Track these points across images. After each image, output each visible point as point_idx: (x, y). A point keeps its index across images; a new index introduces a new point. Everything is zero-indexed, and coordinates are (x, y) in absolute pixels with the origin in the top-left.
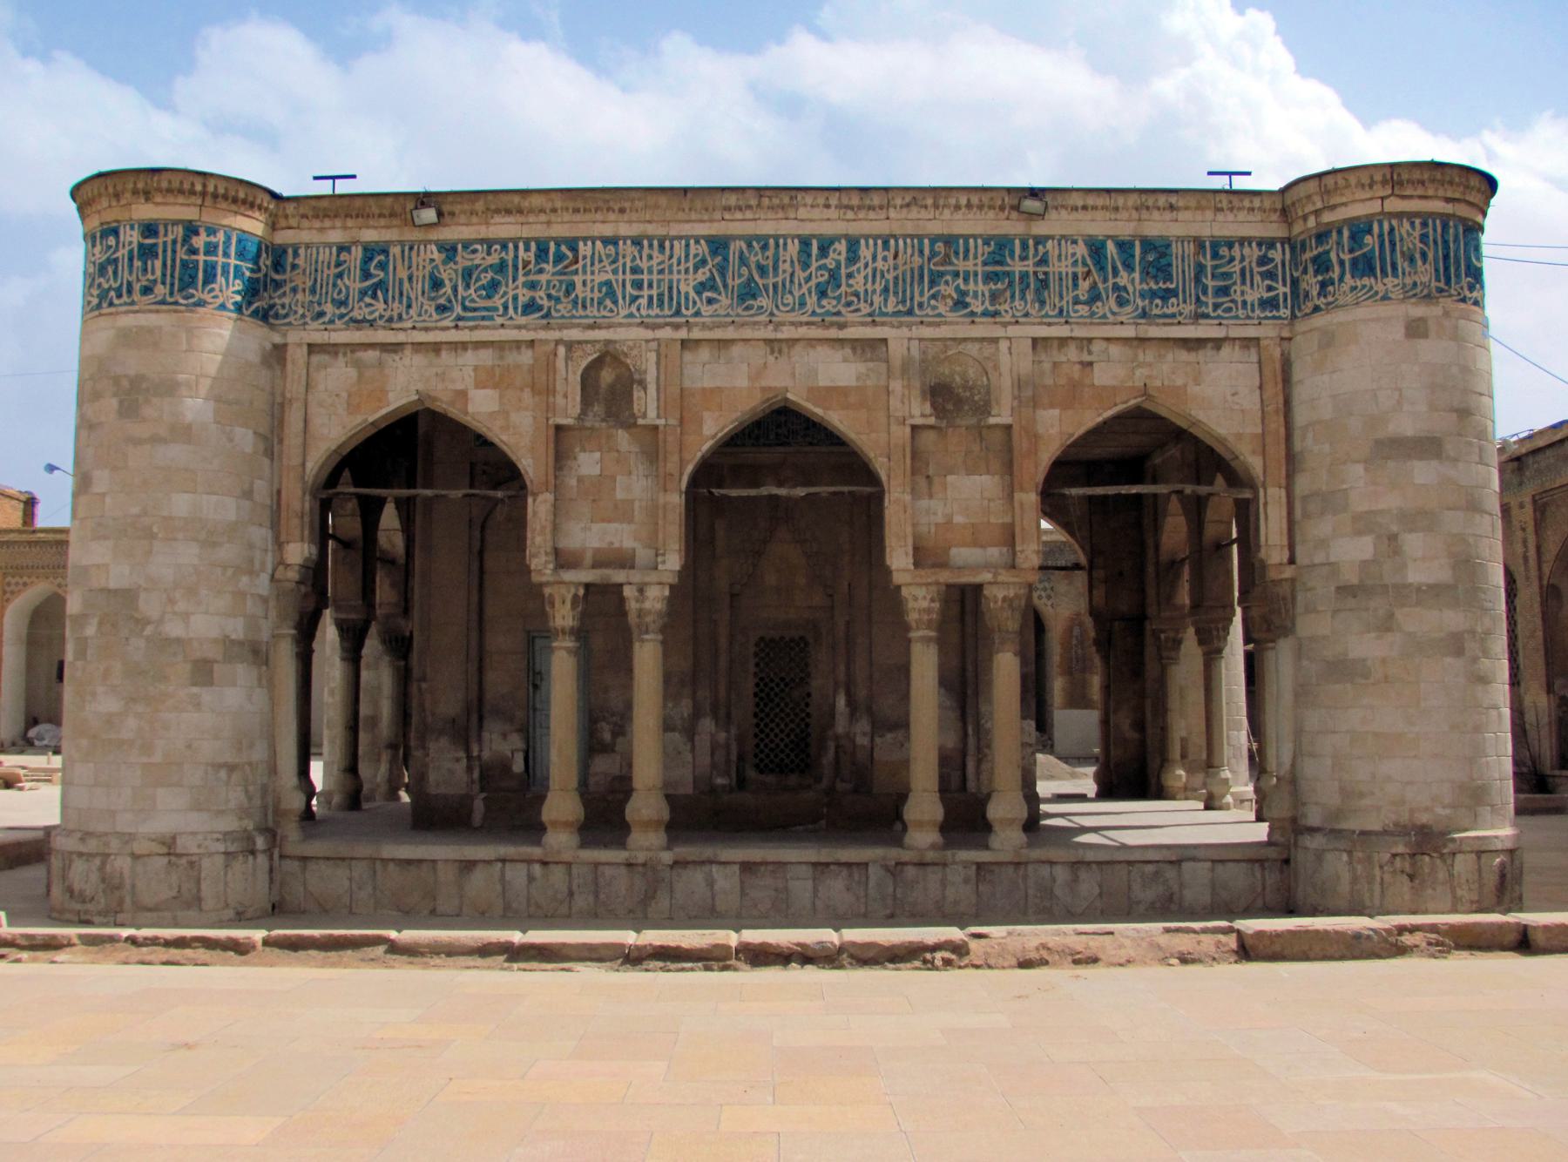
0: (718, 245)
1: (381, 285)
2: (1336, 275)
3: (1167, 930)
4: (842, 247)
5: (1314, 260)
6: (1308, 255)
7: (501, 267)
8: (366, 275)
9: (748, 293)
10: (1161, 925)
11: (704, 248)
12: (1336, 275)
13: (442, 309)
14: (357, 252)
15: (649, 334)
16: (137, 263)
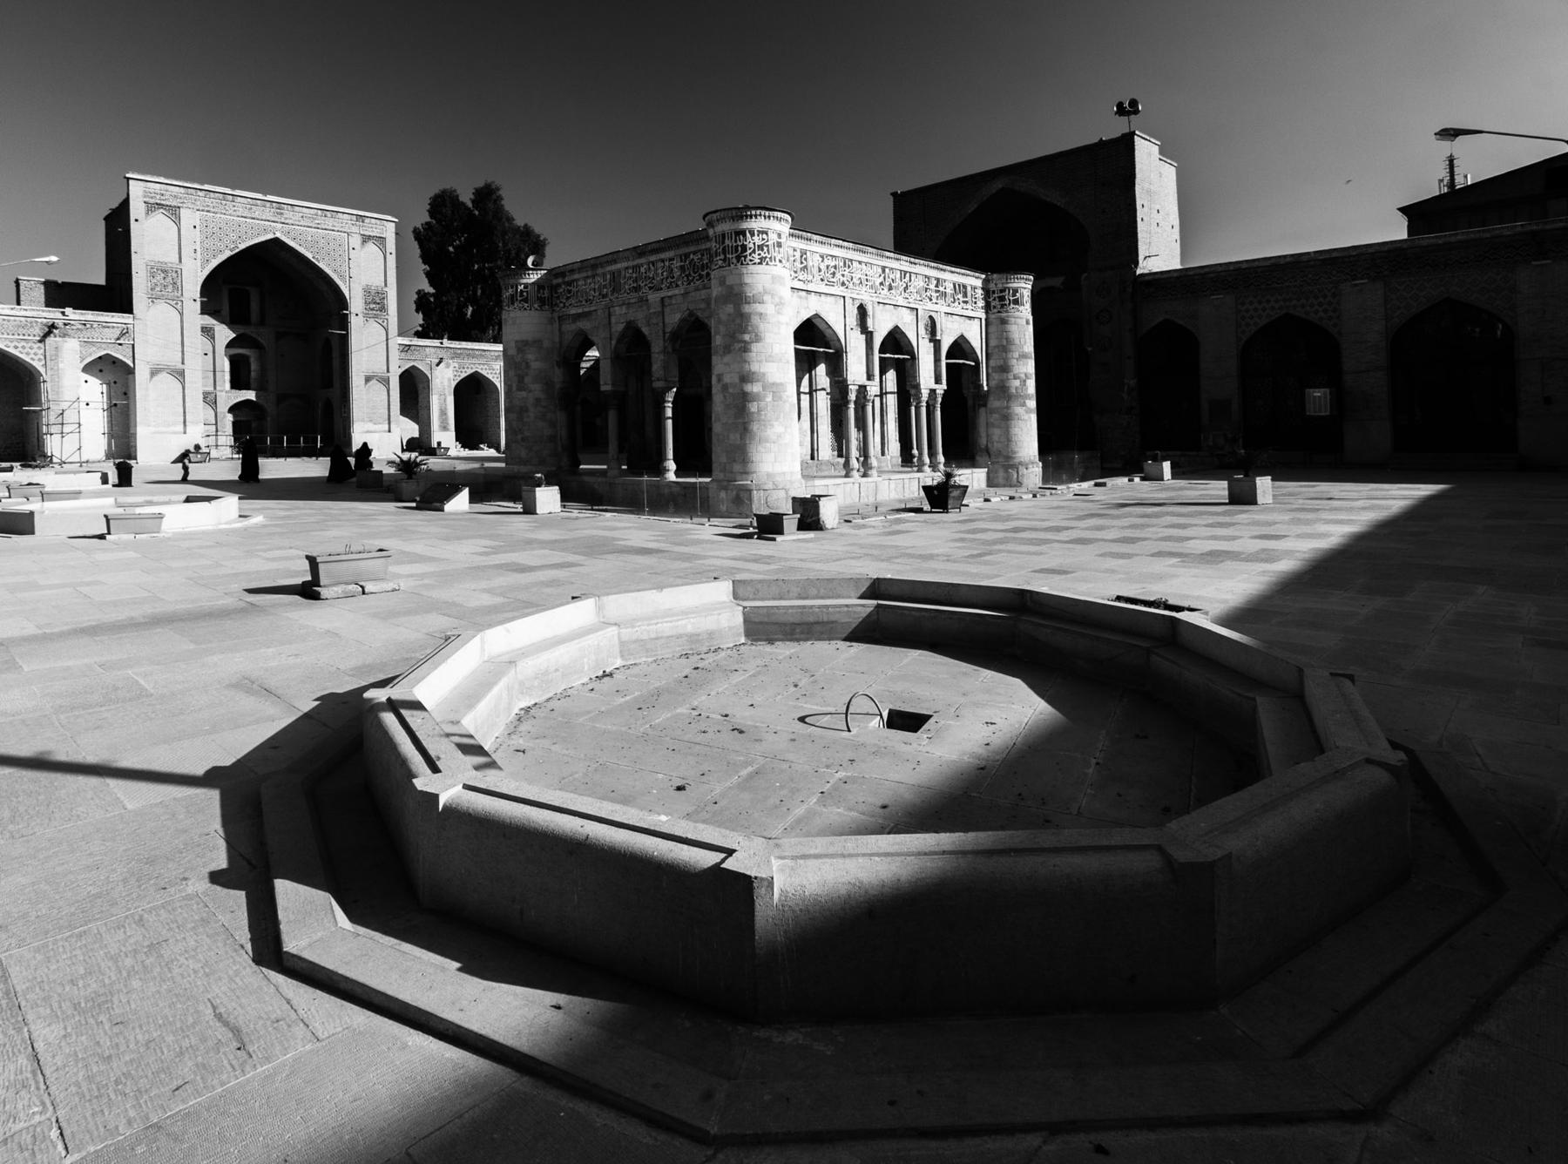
0: (884, 268)
1: (806, 267)
2: (1007, 302)
3: (1096, 485)
4: (908, 275)
5: (999, 297)
6: (996, 295)
7: (835, 267)
8: (802, 263)
9: (890, 288)
10: (1092, 483)
11: (880, 270)
12: (1007, 302)
13: (822, 280)
14: (799, 251)
15: (871, 299)
16: (777, 249)
